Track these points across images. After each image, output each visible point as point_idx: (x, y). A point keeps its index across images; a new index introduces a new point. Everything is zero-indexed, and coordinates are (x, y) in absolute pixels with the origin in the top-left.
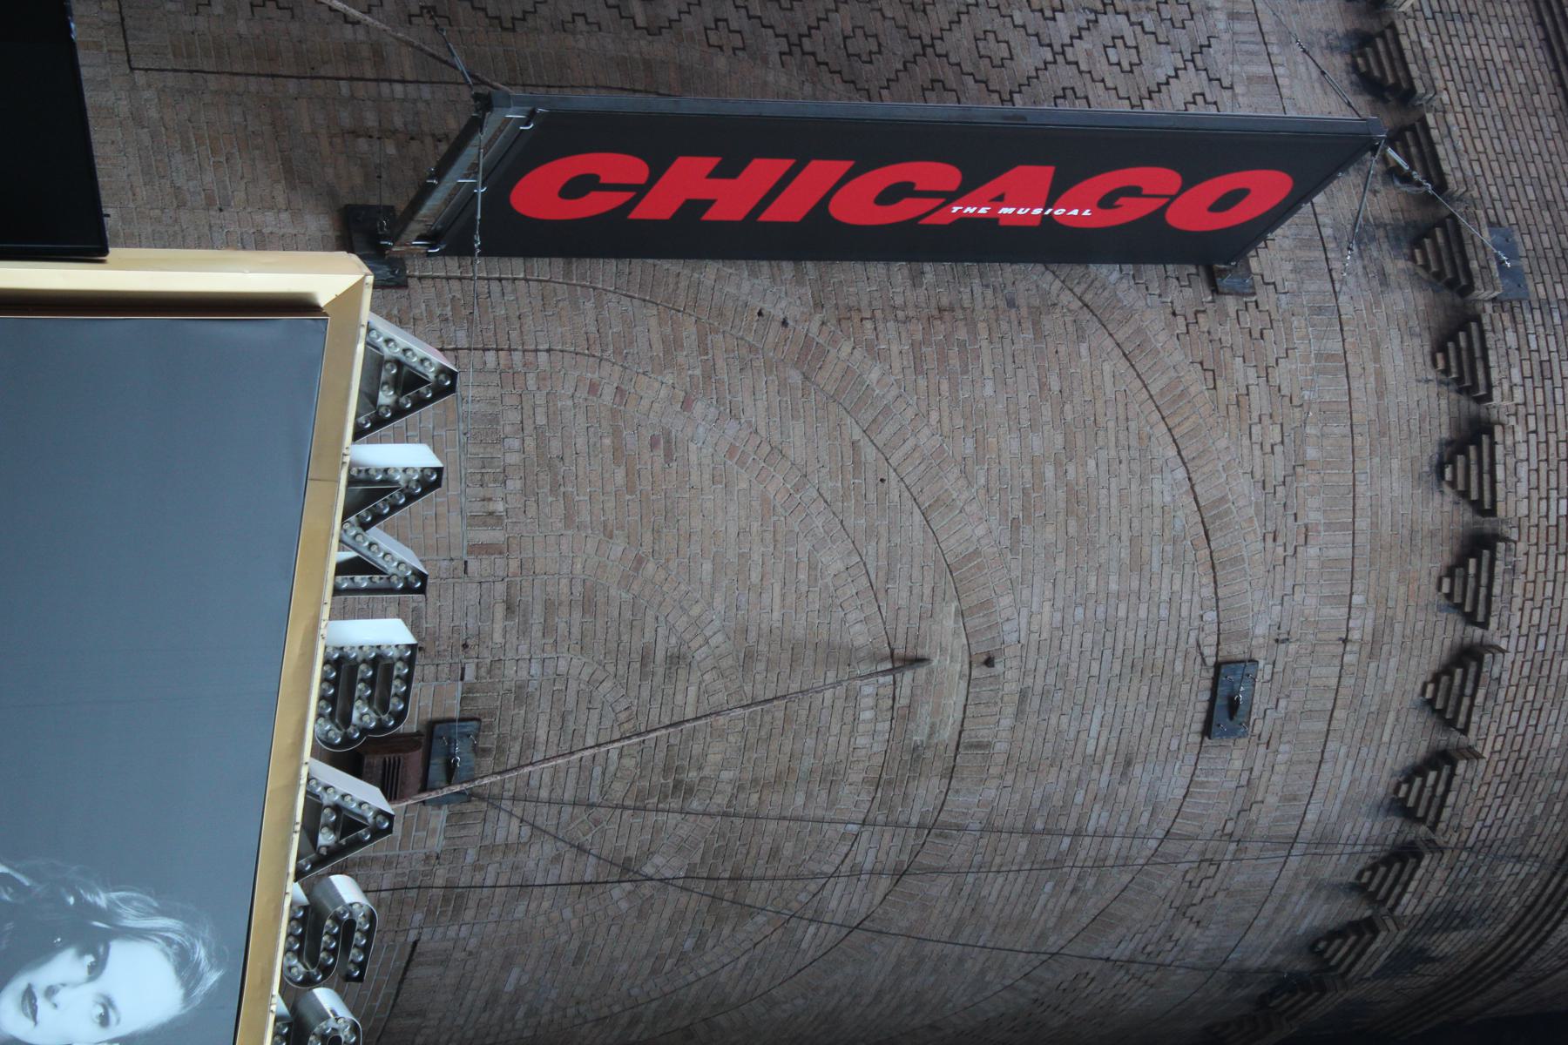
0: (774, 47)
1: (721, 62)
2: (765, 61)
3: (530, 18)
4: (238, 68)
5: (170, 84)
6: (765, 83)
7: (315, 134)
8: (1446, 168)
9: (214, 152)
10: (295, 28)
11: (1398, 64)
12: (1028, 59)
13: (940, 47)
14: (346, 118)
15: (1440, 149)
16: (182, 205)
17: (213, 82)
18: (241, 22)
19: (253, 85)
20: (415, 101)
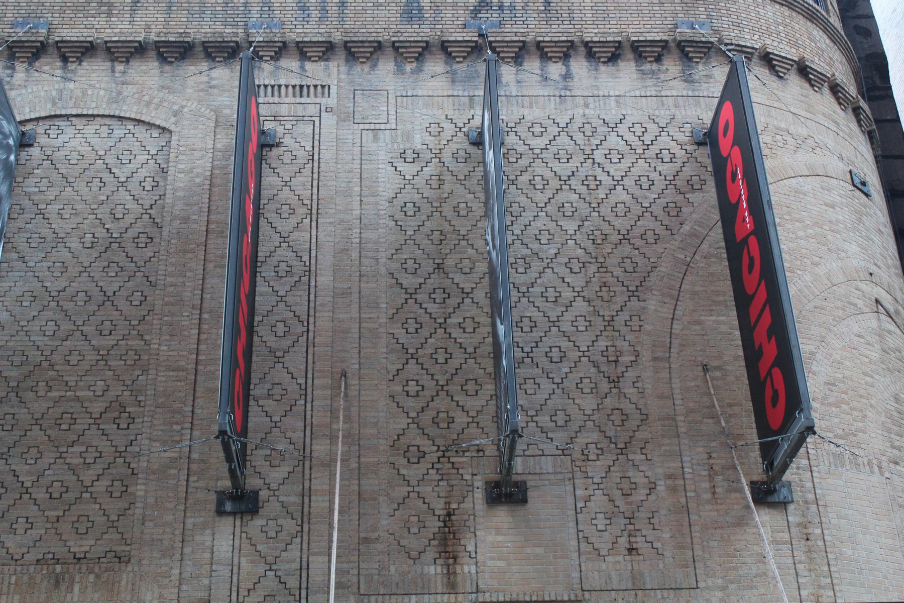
0: (634, 303)
1: (648, 327)
2: (644, 308)
3: (639, 407)
4: (689, 540)
5: (702, 572)
6: (655, 310)
7: (717, 510)
8: (658, 38)
9: (735, 556)
10: (663, 512)
11: (607, 45)
12: (620, 195)
13: (623, 232)
14: (708, 496)
15: (649, 38)
16: (765, 574)
17: (698, 552)
18: (664, 535)
19: (696, 535)
20: (693, 464)
